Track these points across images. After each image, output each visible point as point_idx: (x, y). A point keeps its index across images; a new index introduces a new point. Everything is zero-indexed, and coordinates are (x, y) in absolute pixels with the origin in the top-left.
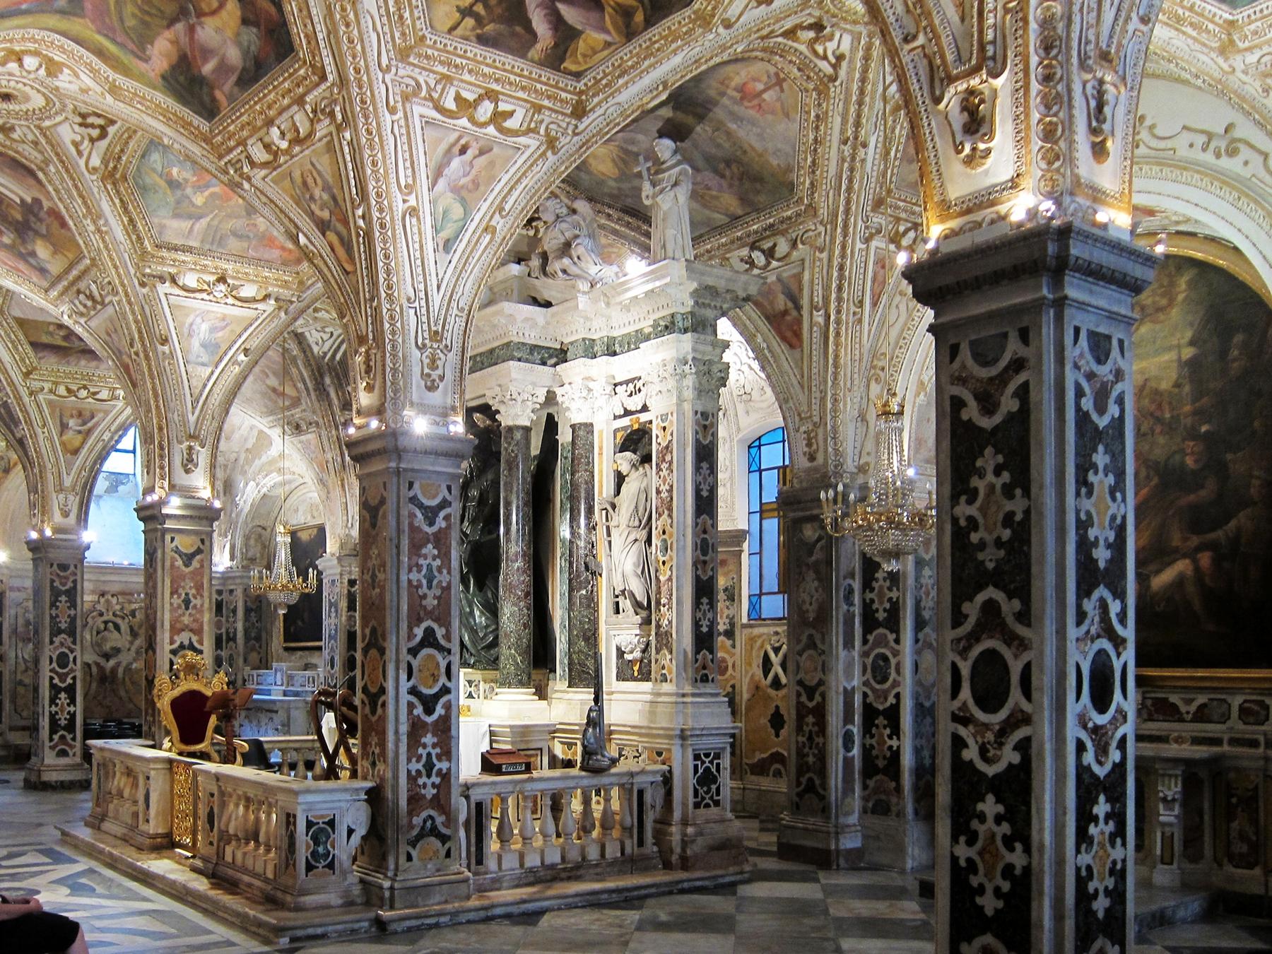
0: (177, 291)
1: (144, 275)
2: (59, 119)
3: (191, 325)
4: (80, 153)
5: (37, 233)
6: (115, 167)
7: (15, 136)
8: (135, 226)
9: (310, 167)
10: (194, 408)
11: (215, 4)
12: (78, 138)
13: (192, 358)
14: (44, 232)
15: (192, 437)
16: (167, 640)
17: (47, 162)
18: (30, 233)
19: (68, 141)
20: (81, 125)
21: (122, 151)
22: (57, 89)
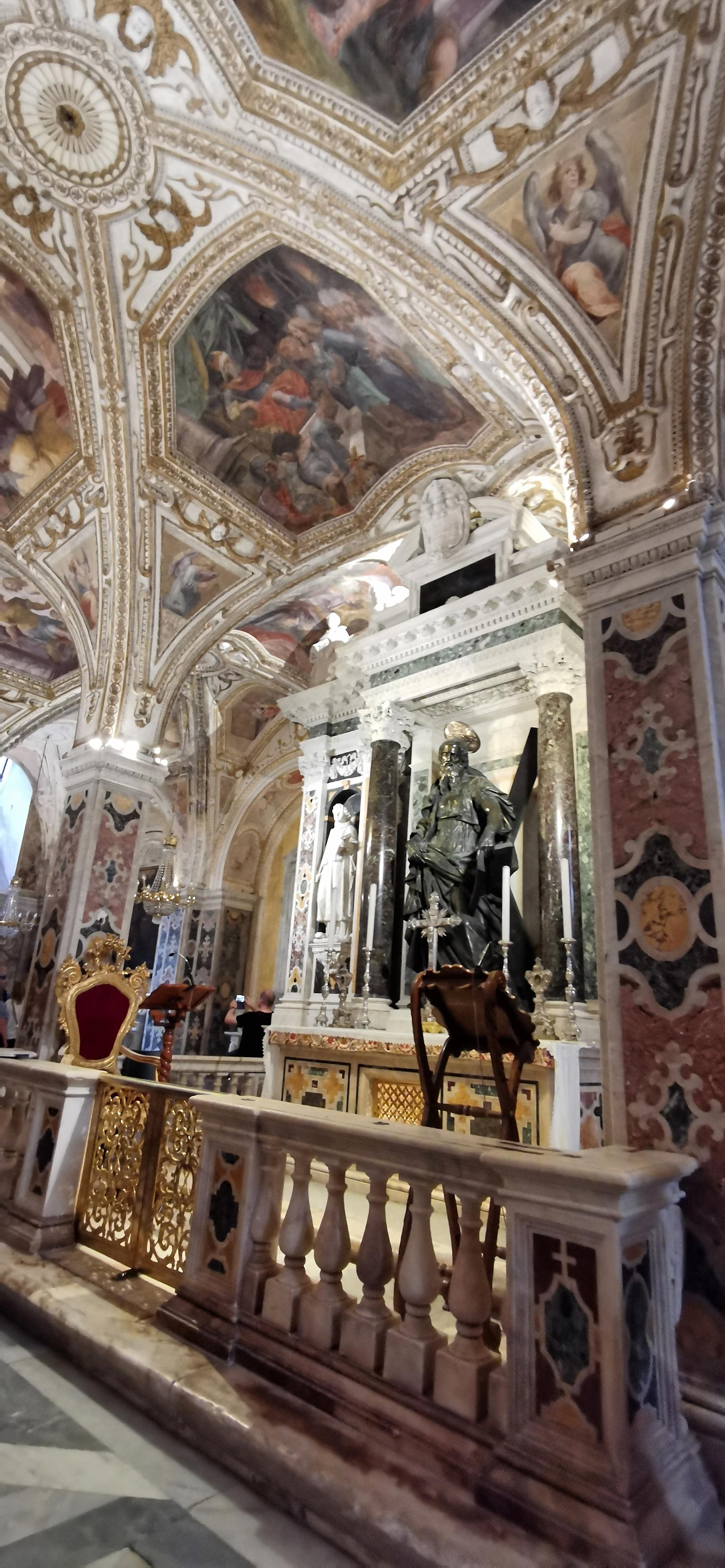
0: (175, 519)
1: (147, 485)
2: (122, 205)
3: (178, 564)
4: (127, 278)
6: (161, 321)
8: (157, 416)
9: (581, 149)
10: (158, 658)
12: (132, 254)
13: (169, 602)
14: (31, 427)
15: (150, 688)
16: (80, 915)
17: (76, 291)
18: (11, 431)
20: (143, 228)
21: (177, 297)
22: (149, 109)
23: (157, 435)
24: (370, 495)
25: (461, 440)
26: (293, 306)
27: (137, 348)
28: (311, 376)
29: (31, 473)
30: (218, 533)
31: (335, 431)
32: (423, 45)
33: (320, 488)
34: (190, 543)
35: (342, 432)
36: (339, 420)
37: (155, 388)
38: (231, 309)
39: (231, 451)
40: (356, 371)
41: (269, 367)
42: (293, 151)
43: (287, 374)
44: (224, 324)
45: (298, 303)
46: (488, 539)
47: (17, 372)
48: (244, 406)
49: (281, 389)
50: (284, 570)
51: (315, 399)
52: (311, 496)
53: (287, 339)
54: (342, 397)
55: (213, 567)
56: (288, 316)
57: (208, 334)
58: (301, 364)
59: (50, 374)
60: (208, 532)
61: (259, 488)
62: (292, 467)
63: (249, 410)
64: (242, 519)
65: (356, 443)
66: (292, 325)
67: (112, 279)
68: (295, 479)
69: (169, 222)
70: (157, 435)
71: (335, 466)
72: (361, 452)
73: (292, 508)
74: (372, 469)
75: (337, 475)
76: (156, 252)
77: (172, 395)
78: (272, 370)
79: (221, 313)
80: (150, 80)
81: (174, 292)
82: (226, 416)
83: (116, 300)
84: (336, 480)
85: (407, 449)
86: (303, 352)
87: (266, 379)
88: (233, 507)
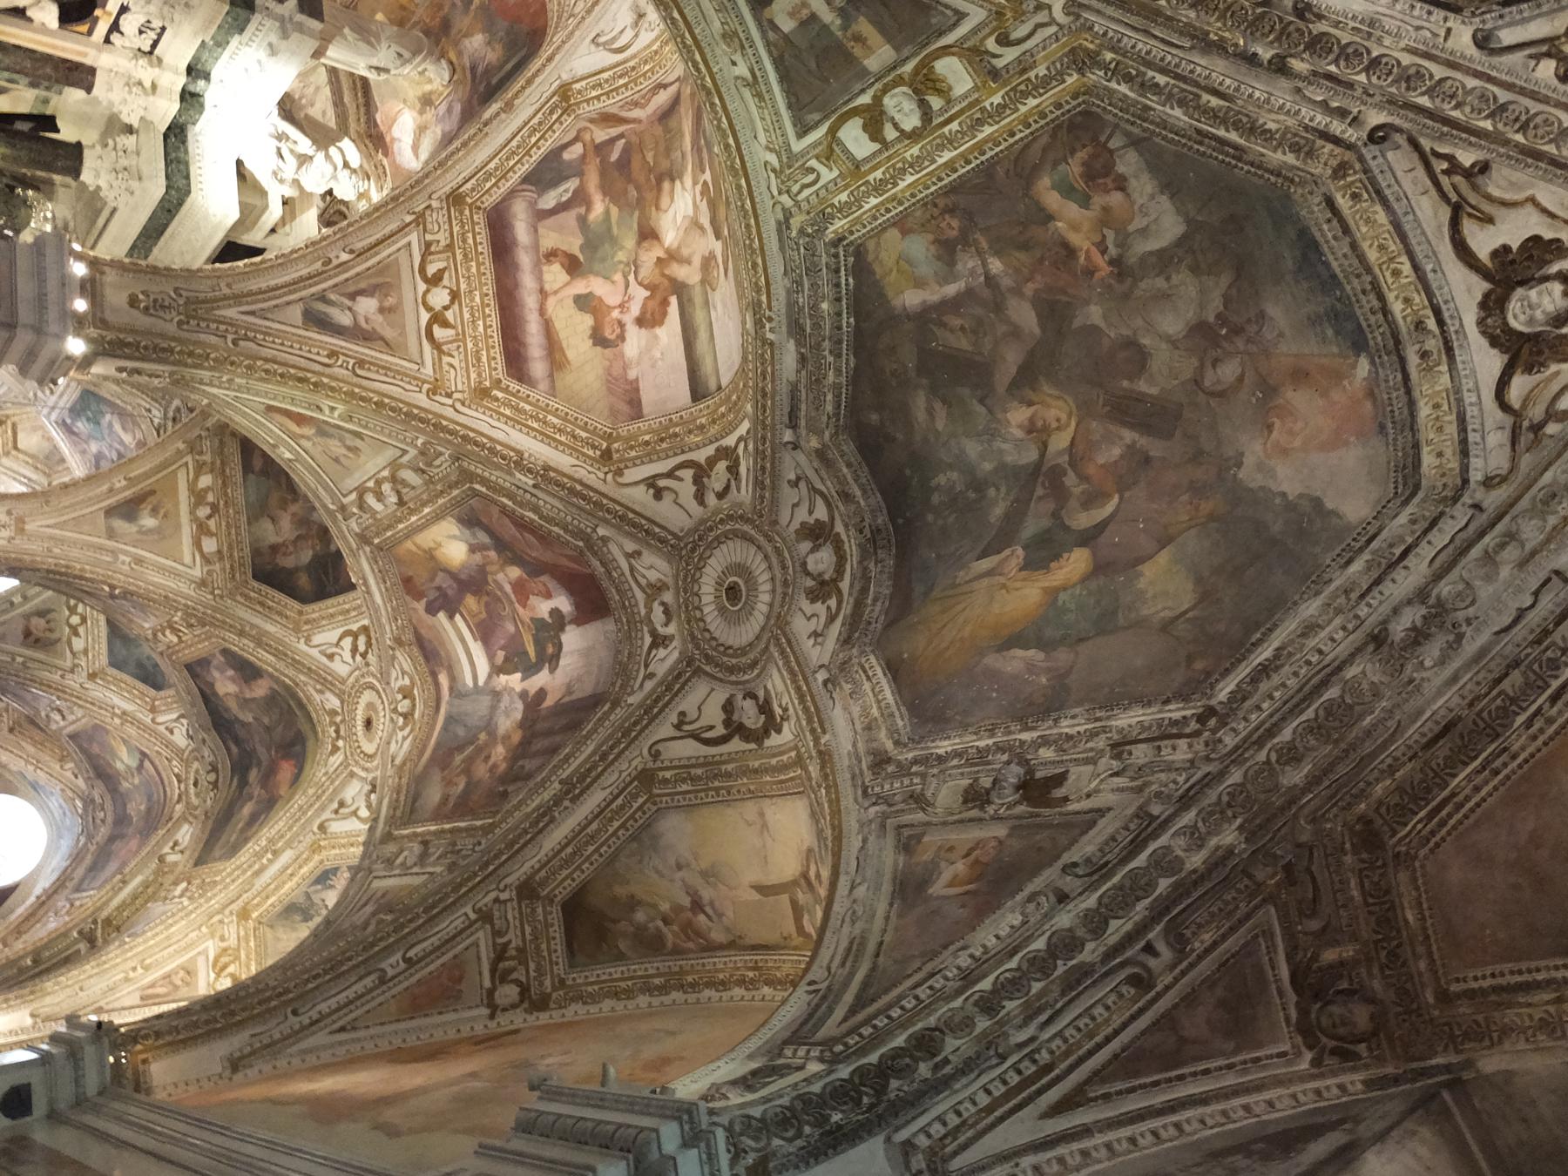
5: (452, 575)
7: (407, 681)
14: (441, 574)
18: (463, 577)
29: (439, 539)
47: (451, 617)
59: (420, 606)
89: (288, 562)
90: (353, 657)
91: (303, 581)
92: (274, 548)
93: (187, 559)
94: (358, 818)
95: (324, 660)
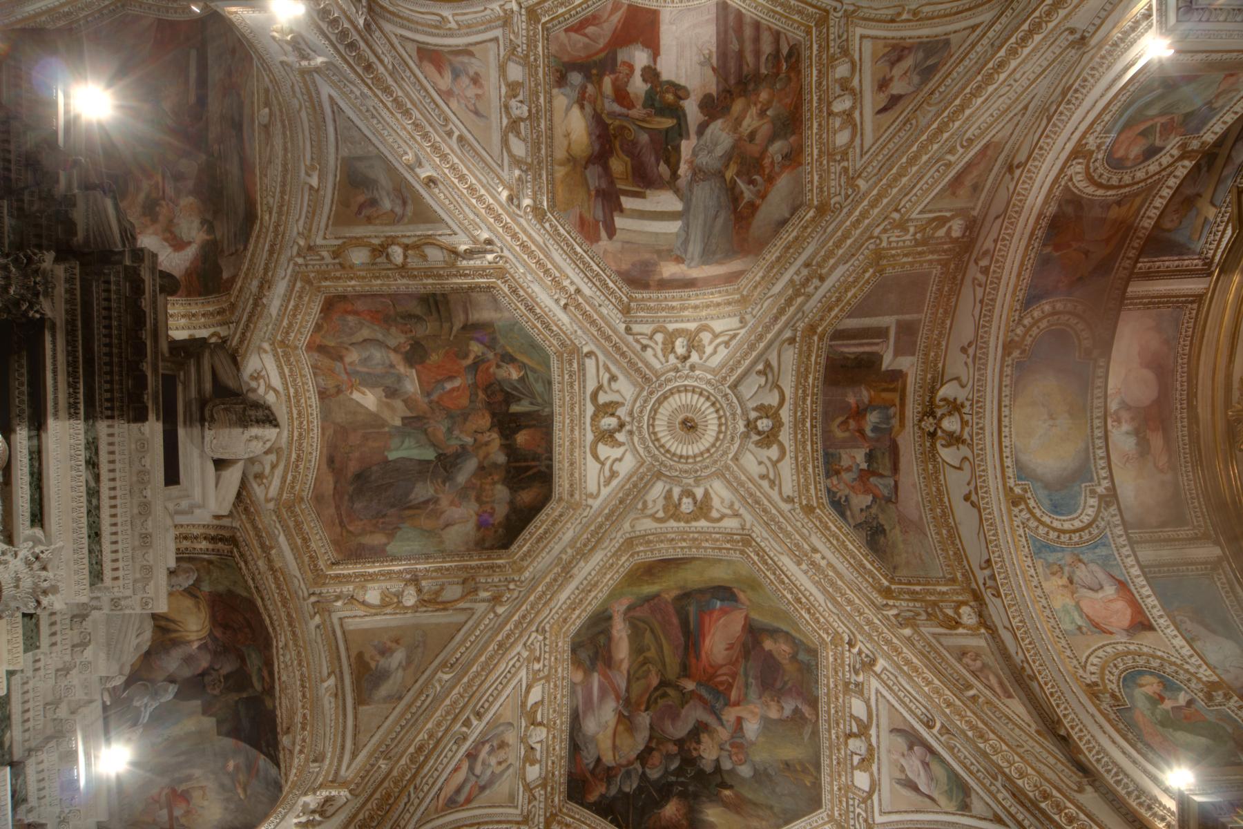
4: (608, 369)
8: (527, 306)
11: (618, 742)
12: (614, 386)
19: (621, 377)
20: (617, 404)
23: (515, 291)
24: (307, 371)
25: (318, 499)
26: (508, 455)
27: (573, 337)
28: (450, 416)
30: (397, 253)
31: (392, 393)
32: (588, 663)
33: (352, 344)
34: (411, 227)
35: (386, 397)
36: (398, 404)
37: (543, 323)
38: (536, 408)
39: (449, 319)
40: (430, 454)
41: (481, 395)
42: (598, 557)
43: (465, 401)
44: (532, 395)
45: (509, 462)
46: (197, 475)
47: (622, 210)
48: (472, 356)
49: (458, 388)
50: (300, 261)
51: (431, 402)
52: (352, 334)
53: (488, 424)
54: (415, 423)
55: (369, 220)
56: (504, 442)
57: (537, 381)
58: (465, 417)
60: (406, 247)
61: (399, 309)
62: (392, 343)
63: (466, 356)
64: (388, 277)
65: (369, 399)
66: (495, 438)
67: (616, 362)
68: (380, 337)
69: (608, 422)
70: (515, 291)
71: (359, 369)
72: (356, 396)
73: (356, 313)
74: (333, 391)
75: (351, 364)
76: (603, 398)
77: (528, 327)
78: (477, 395)
79: (540, 400)
80: (667, 487)
81: (576, 387)
82: (477, 340)
83: (607, 354)
84: (348, 360)
85: (330, 432)
86: (471, 425)
87: (475, 385)
88: (405, 281)
89: (501, 511)
90: (621, 444)
91: (526, 496)
92: (481, 525)
93: (461, 617)
94: (779, 460)
95: (615, 483)
